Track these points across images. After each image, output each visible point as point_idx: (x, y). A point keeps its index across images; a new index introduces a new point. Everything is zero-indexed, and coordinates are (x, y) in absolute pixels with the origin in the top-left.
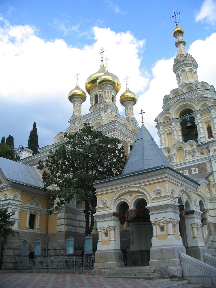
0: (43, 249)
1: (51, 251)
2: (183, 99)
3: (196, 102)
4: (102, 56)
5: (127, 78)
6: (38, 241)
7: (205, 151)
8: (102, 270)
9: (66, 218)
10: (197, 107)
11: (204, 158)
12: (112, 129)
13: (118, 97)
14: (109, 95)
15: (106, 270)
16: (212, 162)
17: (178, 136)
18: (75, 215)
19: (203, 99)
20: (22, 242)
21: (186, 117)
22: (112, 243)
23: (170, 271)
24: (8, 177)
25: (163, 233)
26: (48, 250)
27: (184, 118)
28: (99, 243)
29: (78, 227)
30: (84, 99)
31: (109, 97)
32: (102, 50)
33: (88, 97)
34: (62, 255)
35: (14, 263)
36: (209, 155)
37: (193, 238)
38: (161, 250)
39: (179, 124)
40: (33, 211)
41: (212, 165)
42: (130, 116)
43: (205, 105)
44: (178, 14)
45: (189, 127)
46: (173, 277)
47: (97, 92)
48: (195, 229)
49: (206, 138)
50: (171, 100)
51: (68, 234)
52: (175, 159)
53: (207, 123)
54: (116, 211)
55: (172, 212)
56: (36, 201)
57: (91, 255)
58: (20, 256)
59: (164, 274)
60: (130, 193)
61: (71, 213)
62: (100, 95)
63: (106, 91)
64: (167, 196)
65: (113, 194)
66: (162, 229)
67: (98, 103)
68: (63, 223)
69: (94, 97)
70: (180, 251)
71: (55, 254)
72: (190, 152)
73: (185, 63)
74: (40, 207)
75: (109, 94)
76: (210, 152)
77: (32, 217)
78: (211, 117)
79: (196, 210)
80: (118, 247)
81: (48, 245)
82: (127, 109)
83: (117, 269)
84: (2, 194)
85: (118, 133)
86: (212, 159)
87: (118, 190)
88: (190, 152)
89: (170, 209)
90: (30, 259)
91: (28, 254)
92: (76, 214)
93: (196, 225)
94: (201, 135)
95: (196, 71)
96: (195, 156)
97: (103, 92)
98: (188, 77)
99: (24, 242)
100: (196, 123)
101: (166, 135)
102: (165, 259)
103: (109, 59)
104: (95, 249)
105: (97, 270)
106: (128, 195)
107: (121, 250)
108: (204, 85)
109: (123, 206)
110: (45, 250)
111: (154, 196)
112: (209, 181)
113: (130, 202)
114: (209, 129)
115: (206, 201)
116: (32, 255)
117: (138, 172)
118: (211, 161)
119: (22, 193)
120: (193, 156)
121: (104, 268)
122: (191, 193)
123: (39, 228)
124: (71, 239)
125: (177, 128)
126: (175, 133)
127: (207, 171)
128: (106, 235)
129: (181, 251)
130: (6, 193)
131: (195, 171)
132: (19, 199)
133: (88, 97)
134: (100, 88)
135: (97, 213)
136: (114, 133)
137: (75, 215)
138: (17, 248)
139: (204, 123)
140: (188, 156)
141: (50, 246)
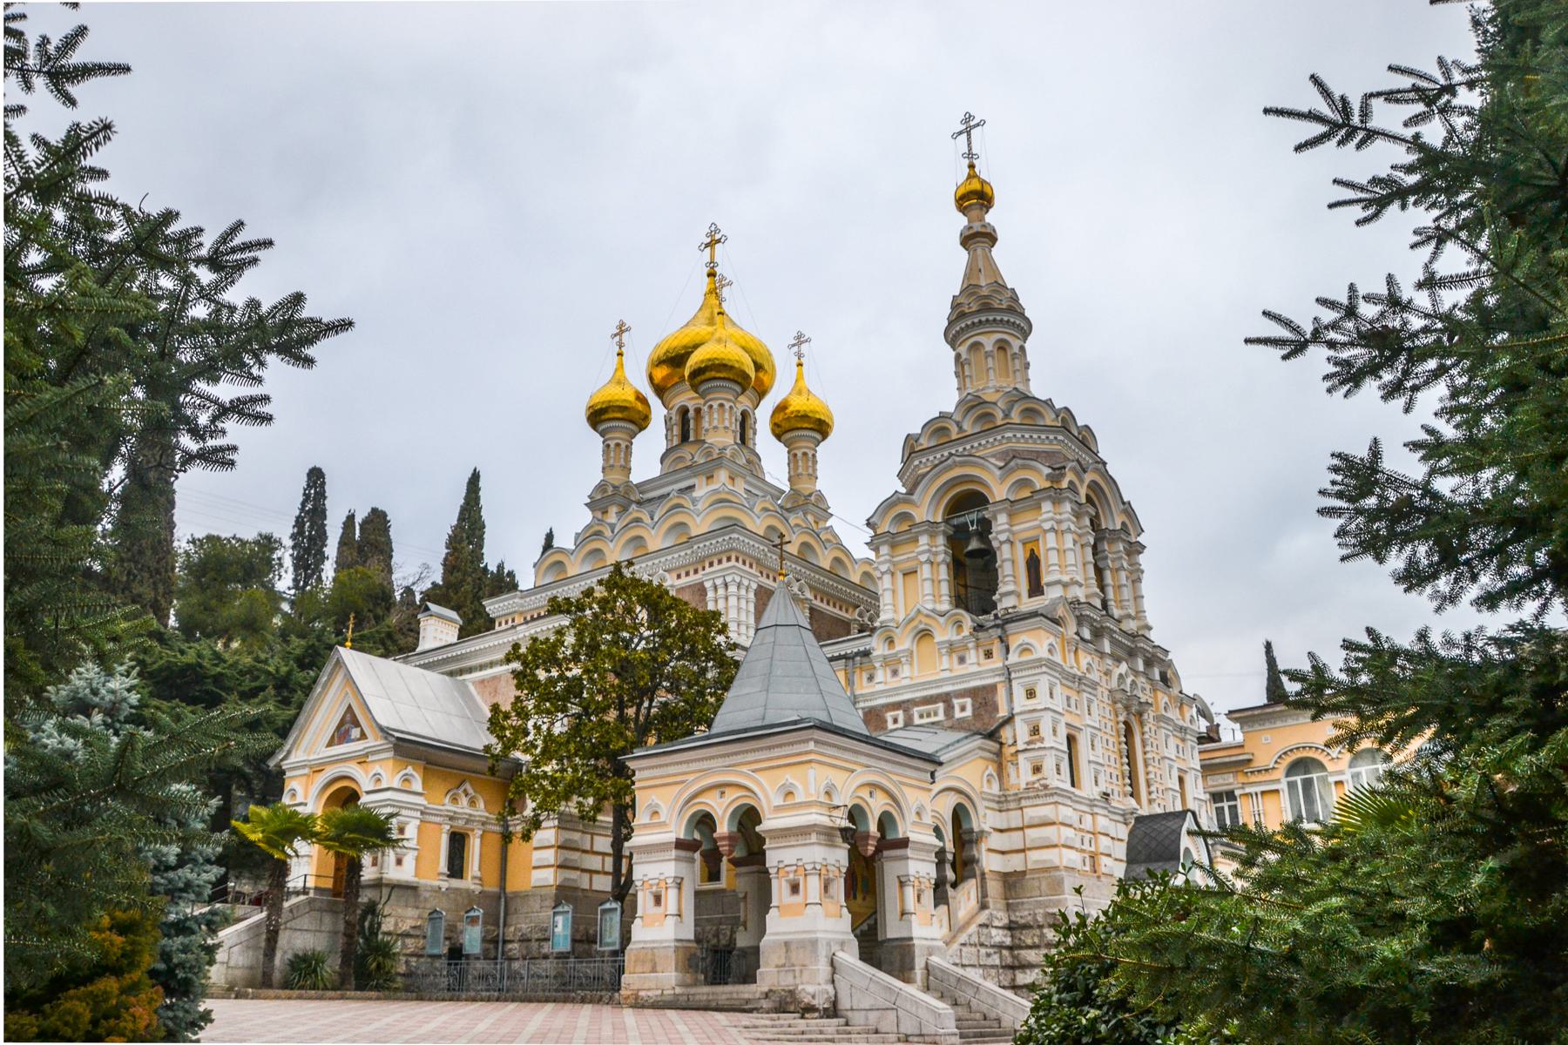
0: (489, 937)
1: (516, 945)
2: (958, 459)
3: (998, 473)
4: (712, 256)
5: (800, 340)
6: (472, 914)
7: (997, 648)
8: (642, 993)
9: (559, 847)
10: (999, 491)
11: (992, 670)
12: (721, 552)
13: (763, 415)
14: (723, 420)
15: (650, 993)
16: (1014, 683)
17: (935, 582)
18: (589, 837)
19: (1020, 462)
20: (426, 915)
21: (968, 519)
22: (671, 921)
23: (803, 995)
24: (383, 722)
25: (798, 899)
26: (505, 942)
27: (962, 520)
28: (637, 921)
29: (597, 872)
30: (637, 420)
31: (726, 428)
32: (710, 234)
33: (658, 411)
34: (546, 957)
35: (404, 975)
36: (1007, 663)
37: (903, 914)
38: (787, 944)
39: (941, 540)
40: (461, 823)
41: (1011, 694)
42: (805, 487)
43: (1024, 483)
44: (978, 125)
45: (973, 554)
46: (810, 1009)
47: (686, 398)
48: (910, 893)
49: (1019, 596)
50: (922, 456)
51: (564, 894)
52: (906, 668)
53: (1029, 546)
54: (686, 834)
55: (820, 844)
56: (471, 791)
57: (615, 953)
58: (422, 956)
59: (787, 1003)
60: (722, 788)
61: (577, 831)
62: (698, 411)
63: (715, 405)
64: (807, 804)
65: (677, 789)
66: (795, 888)
67: (691, 439)
68: (552, 861)
69: (676, 418)
70: (835, 948)
71: (525, 952)
72: (951, 647)
73: (983, 319)
74: (481, 810)
75: (727, 415)
76: (1012, 649)
77: (458, 842)
78: (1039, 527)
79: (913, 837)
80: (689, 933)
81: (505, 925)
82: (793, 458)
83: (678, 990)
84: (367, 772)
85: (744, 563)
86: (1013, 675)
87: (691, 777)
88: (951, 647)
89: (814, 838)
90: (449, 964)
91: (445, 951)
92: (592, 834)
93: (912, 879)
94: (1004, 583)
95: (1022, 349)
96: (968, 661)
97: (705, 408)
98: (991, 372)
99: (434, 916)
100: (995, 544)
101: (899, 576)
102: (793, 965)
103: (730, 284)
104: (626, 938)
105: (629, 993)
106: (716, 793)
107: (698, 940)
108: (1032, 408)
109: (704, 821)
110: (497, 942)
111: (779, 801)
112: (1001, 744)
113: (720, 813)
114: (1033, 564)
115: (980, 805)
116: (456, 953)
117: (746, 731)
118: (1010, 681)
119: (425, 768)
120: (962, 660)
121: (646, 986)
122: (903, 787)
123: (478, 874)
124: (566, 908)
125: (936, 554)
126: (926, 571)
127: (996, 709)
128: (658, 900)
129: (837, 947)
130: (377, 768)
131: (963, 709)
132: (417, 785)
133: (658, 411)
134: (695, 388)
135: (637, 839)
136: (730, 564)
137: (589, 837)
138: (412, 932)
139: (1019, 546)
140: (945, 659)
141: (512, 929)
